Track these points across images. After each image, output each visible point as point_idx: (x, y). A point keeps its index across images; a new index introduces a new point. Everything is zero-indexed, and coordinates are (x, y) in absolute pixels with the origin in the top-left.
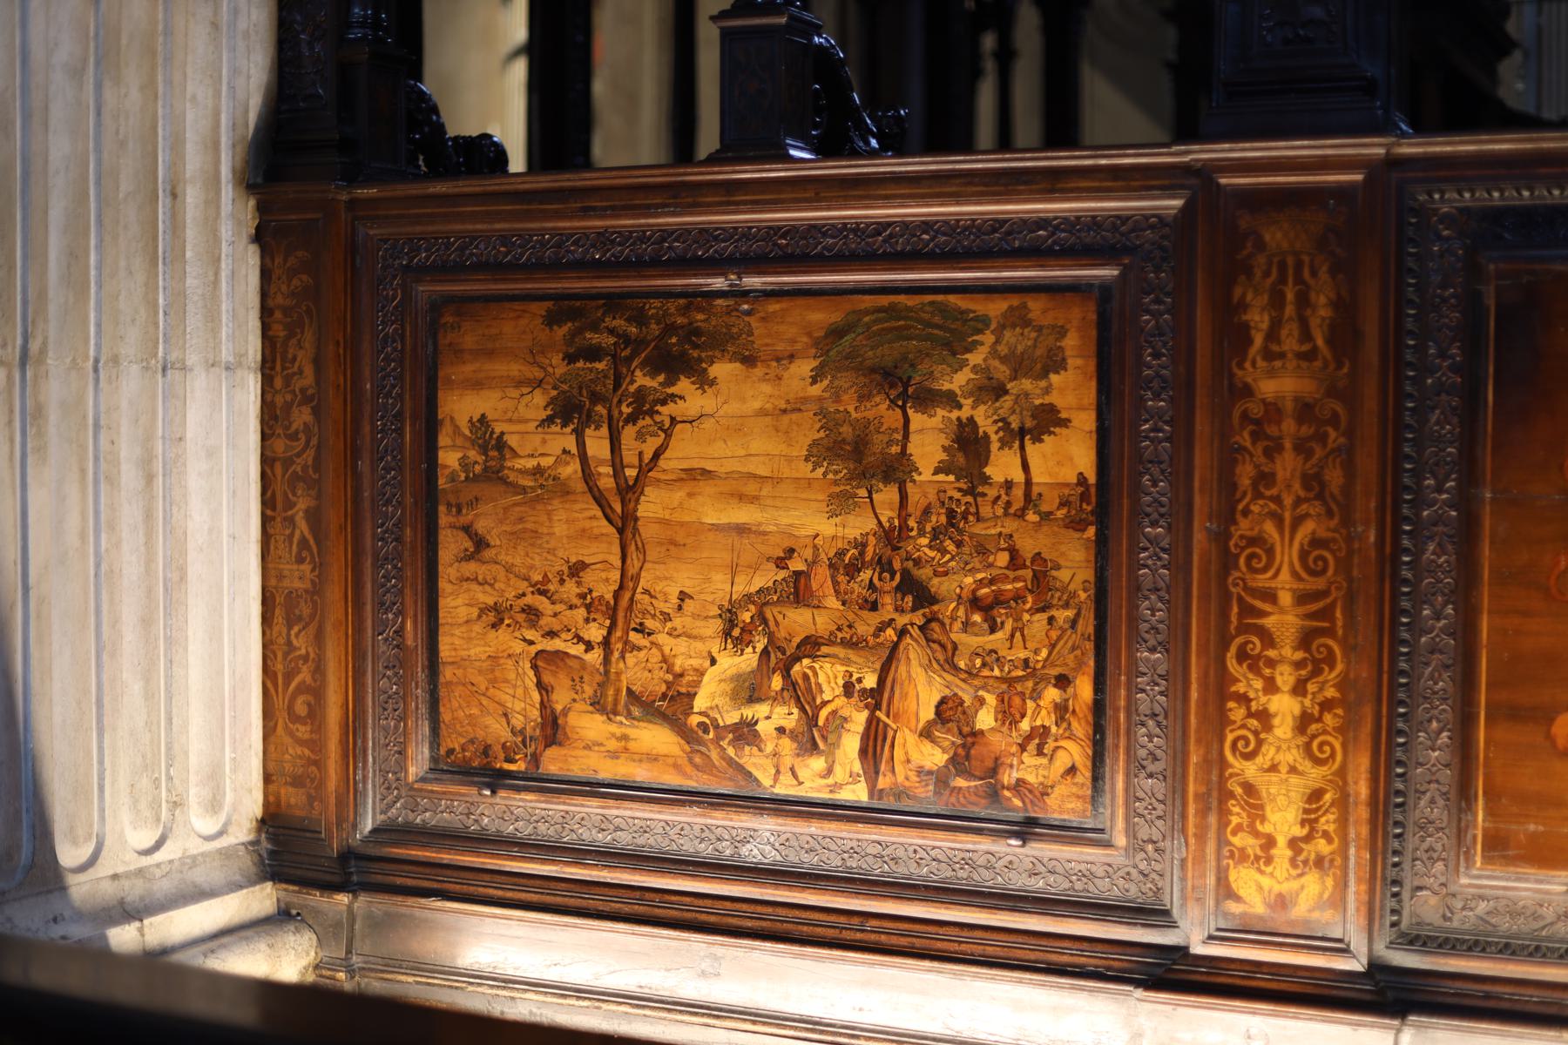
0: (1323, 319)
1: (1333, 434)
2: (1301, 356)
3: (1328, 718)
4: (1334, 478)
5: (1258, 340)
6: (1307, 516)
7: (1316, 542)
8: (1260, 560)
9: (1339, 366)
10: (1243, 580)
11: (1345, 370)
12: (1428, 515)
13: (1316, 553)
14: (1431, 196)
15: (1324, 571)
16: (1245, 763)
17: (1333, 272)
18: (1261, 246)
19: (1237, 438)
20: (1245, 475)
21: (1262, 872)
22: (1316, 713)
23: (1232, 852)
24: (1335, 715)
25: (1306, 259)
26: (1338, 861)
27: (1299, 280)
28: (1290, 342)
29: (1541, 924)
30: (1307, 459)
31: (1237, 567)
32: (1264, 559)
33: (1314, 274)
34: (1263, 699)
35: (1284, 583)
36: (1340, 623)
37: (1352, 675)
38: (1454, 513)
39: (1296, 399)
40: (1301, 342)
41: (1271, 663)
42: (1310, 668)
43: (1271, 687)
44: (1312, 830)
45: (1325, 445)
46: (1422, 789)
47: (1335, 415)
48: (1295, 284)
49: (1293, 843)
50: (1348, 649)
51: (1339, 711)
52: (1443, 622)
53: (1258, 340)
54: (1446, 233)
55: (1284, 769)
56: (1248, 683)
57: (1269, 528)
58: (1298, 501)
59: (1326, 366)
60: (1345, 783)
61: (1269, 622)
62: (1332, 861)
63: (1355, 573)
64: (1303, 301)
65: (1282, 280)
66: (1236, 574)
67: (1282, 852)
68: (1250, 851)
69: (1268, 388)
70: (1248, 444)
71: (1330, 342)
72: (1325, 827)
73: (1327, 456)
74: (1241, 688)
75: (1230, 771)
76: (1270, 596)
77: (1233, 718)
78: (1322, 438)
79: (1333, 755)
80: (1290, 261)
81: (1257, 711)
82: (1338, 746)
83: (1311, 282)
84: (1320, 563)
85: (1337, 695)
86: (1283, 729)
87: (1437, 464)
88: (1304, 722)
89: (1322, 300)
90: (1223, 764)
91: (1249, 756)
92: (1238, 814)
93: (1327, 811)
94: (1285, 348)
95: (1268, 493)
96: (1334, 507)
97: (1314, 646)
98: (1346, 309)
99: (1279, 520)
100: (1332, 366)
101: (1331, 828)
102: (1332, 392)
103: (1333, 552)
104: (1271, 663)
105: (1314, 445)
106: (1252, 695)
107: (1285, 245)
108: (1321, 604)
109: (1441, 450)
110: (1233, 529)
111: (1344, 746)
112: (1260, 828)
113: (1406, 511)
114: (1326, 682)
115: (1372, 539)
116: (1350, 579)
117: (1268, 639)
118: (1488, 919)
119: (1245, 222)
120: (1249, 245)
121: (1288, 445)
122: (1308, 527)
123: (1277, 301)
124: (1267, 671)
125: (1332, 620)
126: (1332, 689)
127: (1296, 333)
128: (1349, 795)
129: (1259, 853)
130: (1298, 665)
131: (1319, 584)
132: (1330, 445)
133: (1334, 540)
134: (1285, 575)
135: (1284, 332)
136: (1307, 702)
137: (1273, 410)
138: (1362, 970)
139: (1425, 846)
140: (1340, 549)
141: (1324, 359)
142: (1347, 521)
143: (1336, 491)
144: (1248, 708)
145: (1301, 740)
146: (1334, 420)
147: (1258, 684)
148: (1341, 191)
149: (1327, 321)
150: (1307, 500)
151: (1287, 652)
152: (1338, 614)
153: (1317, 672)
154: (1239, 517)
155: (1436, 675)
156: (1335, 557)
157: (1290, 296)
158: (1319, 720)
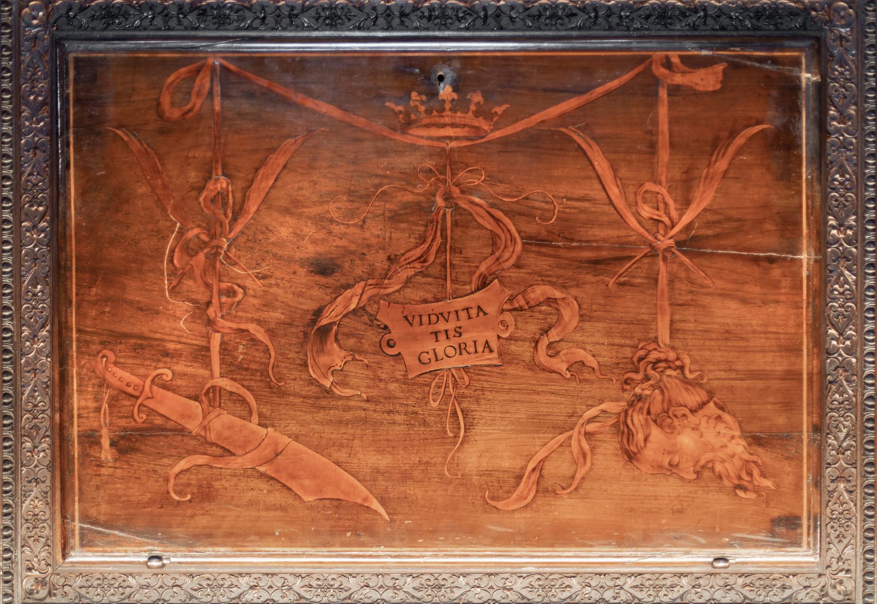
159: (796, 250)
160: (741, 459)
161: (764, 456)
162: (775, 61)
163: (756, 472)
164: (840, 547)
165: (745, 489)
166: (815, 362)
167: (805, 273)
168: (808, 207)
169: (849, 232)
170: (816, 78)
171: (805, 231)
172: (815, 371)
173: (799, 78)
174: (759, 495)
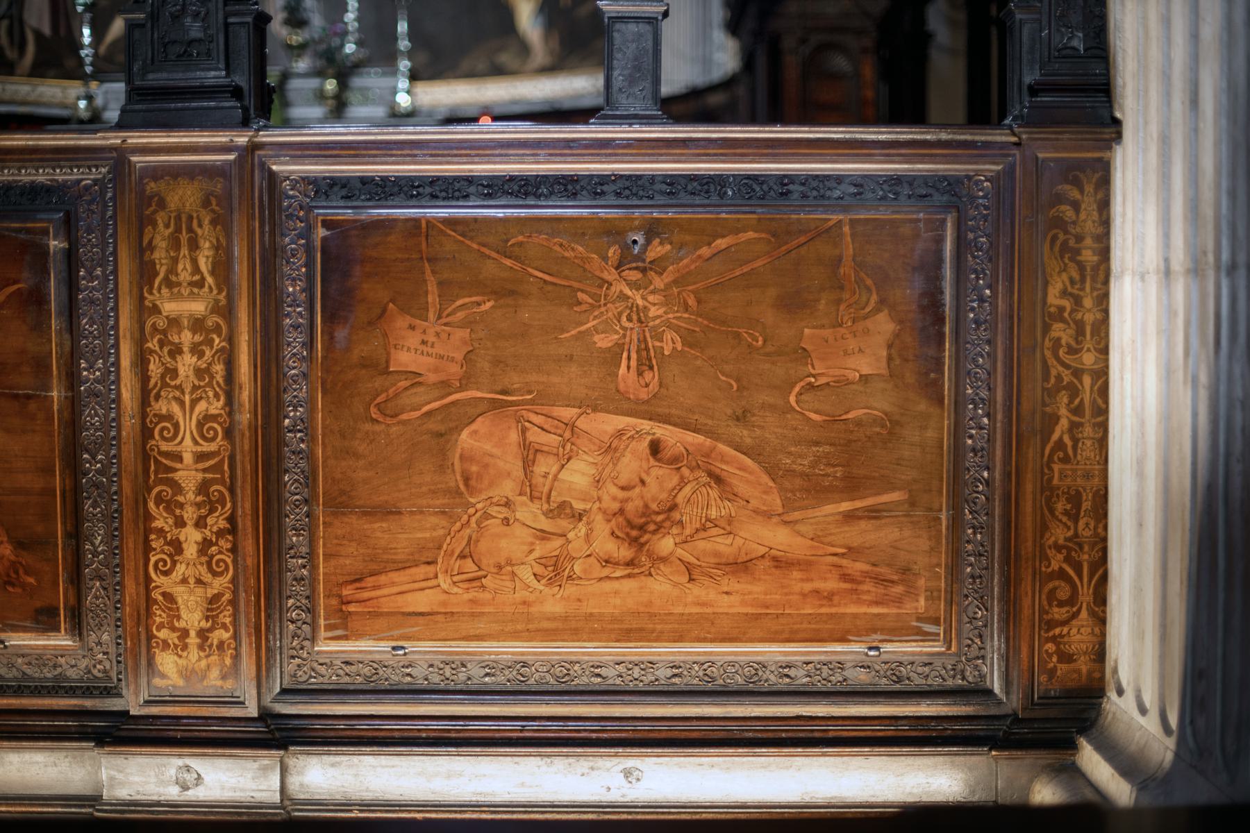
0: (207, 257)
1: (217, 341)
3: (222, 542)
5: (162, 272)
6: (201, 398)
8: (169, 432)
10: (157, 446)
16: (162, 577)
17: (214, 222)
18: (162, 204)
19: (150, 345)
20: (155, 369)
21: (177, 654)
22: (214, 540)
23: (157, 643)
25: (195, 215)
28: (184, 273)
31: (152, 437)
32: (172, 431)
33: (200, 226)
34: (175, 531)
35: (188, 448)
41: (181, 506)
43: (180, 523)
44: (214, 622)
45: (212, 347)
47: (218, 324)
49: (203, 634)
53: (162, 272)
55: (192, 580)
56: (162, 521)
57: (176, 409)
58: (195, 388)
61: (177, 476)
62: (230, 644)
65: (178, 230)
66: (154, 442)
67: (193, 640)
68: (170, 641)
69: (170, 307)
70: (157, 348)
71: (212, 273)
74: (158, 524)
75: (153, 584)
76: (179, 458)
77: (154, 546)
78: (210, 343)
79: (227, 569)
81: (171, 540)
82: (229, 561)
83: (199, 231)
85: (228, 526)
86: (191, 551)
88: (205, 545)
89: (207, 245)
90: (148, 580)
91: (166, 573)
92: (160, 615)
95: (173, 383)
96: (220, 393)
99: (182, 403)
100: (215, 292)
101: (228, 620)
103: (220, 424)
104: (181, 506)
105: (204, 348)
106: (167, 529)
108: (212, 462)
110: (148, 410)
112: (176, 624)
117: (177, 488)
119: (152, 187)
120: (154, 204)
121: (185, 349)
122: (201, 407)
123: (175, 244)
124: (178, 512)
125: (222, 473)
127: (188, 267)
129: (177, 642)
130: (199, 506)
131: (213, 447)
134: (188, 441)
135: (180, 267)
136: (208, 533)
137: (174, 322)
140: (225, 421)
144: (165, 538)
145: (204, 559)
146: (217, 329)
147: (171, 521)
149: (210, 259)
151: (191, 496)
153: (212, 511)
154: (152, 399)
156: (222, 428)
158: (216, 544)
159: (49, 389)
160: (9, 560)
161: (27, 558)
162: (28, 231)
163: (21, 571)
164: (99, 633)
165: (13, 585)
166: (67, 481)
167: (56, 408)
168: (57, 353)
169: (98, 373)
170: (65, 245)
171: (55, 372)
172: (67, 488)
173: (48, 246)
174: (24, 590)
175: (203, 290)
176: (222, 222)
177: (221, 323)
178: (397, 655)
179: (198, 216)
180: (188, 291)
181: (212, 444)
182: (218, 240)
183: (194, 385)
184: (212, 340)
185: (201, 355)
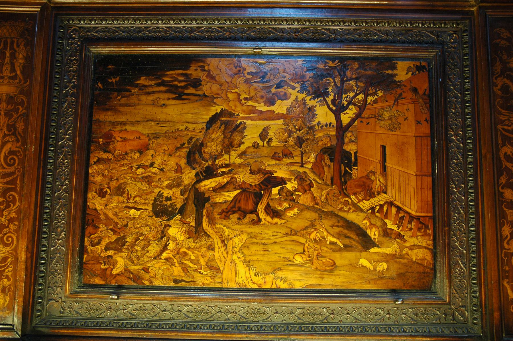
0: (20, 63)
1: (21, 109)
2: (10, 78)
3: (11, 226)
4: (20, 126)
6: (9, 141)
7: (11, 152)
9: (26, 82)
11: (28, 84)
12: (60, 144)
13: (11, 157)
14: (69, 22)
15: (14, 164)
17: (26, 45)
24: (15, 224)
25: (15, 40)
26: (12, 289)
27: (12, 48)
29: (101, 312)
30: (9, 119)
33: (18, 46)
36: (19, 186)
37: (22, 207)
38: (71, 143)
39: (7, 95)
40: (11, 72)
42: (5, 205)
45: (17, 113)
46: (53, 257)
47: (22, 100)
48: (10, 50)
50: (21, 195)
51: (16, 223)
52: (64, 187)
54: (74, 36)
59: (20, 82)
60: (17, 254)
62: (9, 288)
63: (26, 165)
64: (13, 56)
65: (5, 48)
71: (22, 72)
72: (7, 274)
73: (18, 118)
78: (17, 110)
80: (9, 41)
83: (17, 49)
84: (12, 161)
87: (65, 124)
89: (21, 56)
93: (8, 266)
94: (4, 74)
97: (8, 195)
98: (29, 59)
100: (23, 82)
101: (10, 274)
102: (21, 92)
103: (17, 156)
107: (7, 35)
108: (11, 178)
109: (67, 118)
111: (17, 238)
113: (51, 141)
114: (12, 210)
115: (33, 150)
116: (24, 168)
118: (79, 311)
122: (8, 146)
125: (16, 184)
126: (14, 214)
128: (18, 259)
131: (11, 169)
132: (20, 113)
133: (19, 151)
138: (19, 337)
139: (54, 281)
141: (20, 79)
142: (24, 144)
143: (21, 132)
146: (22, 103)
148: (31, 16)
150: (9, 135)
152: (18, 182)
153: (8, 206)
155: (61, 208)
156: (19, 158)
157: (8, 55)
158: (8, 227)
175: (16, 81)
176: (29, 44)
177: (24, 99)
178: (113, 299)
179: (17, 41)
180: (8, 80)
181: (12, 168)
182: (27, 54)
183: (5, 134)
184: (18, 109)
185: (11, 116)
